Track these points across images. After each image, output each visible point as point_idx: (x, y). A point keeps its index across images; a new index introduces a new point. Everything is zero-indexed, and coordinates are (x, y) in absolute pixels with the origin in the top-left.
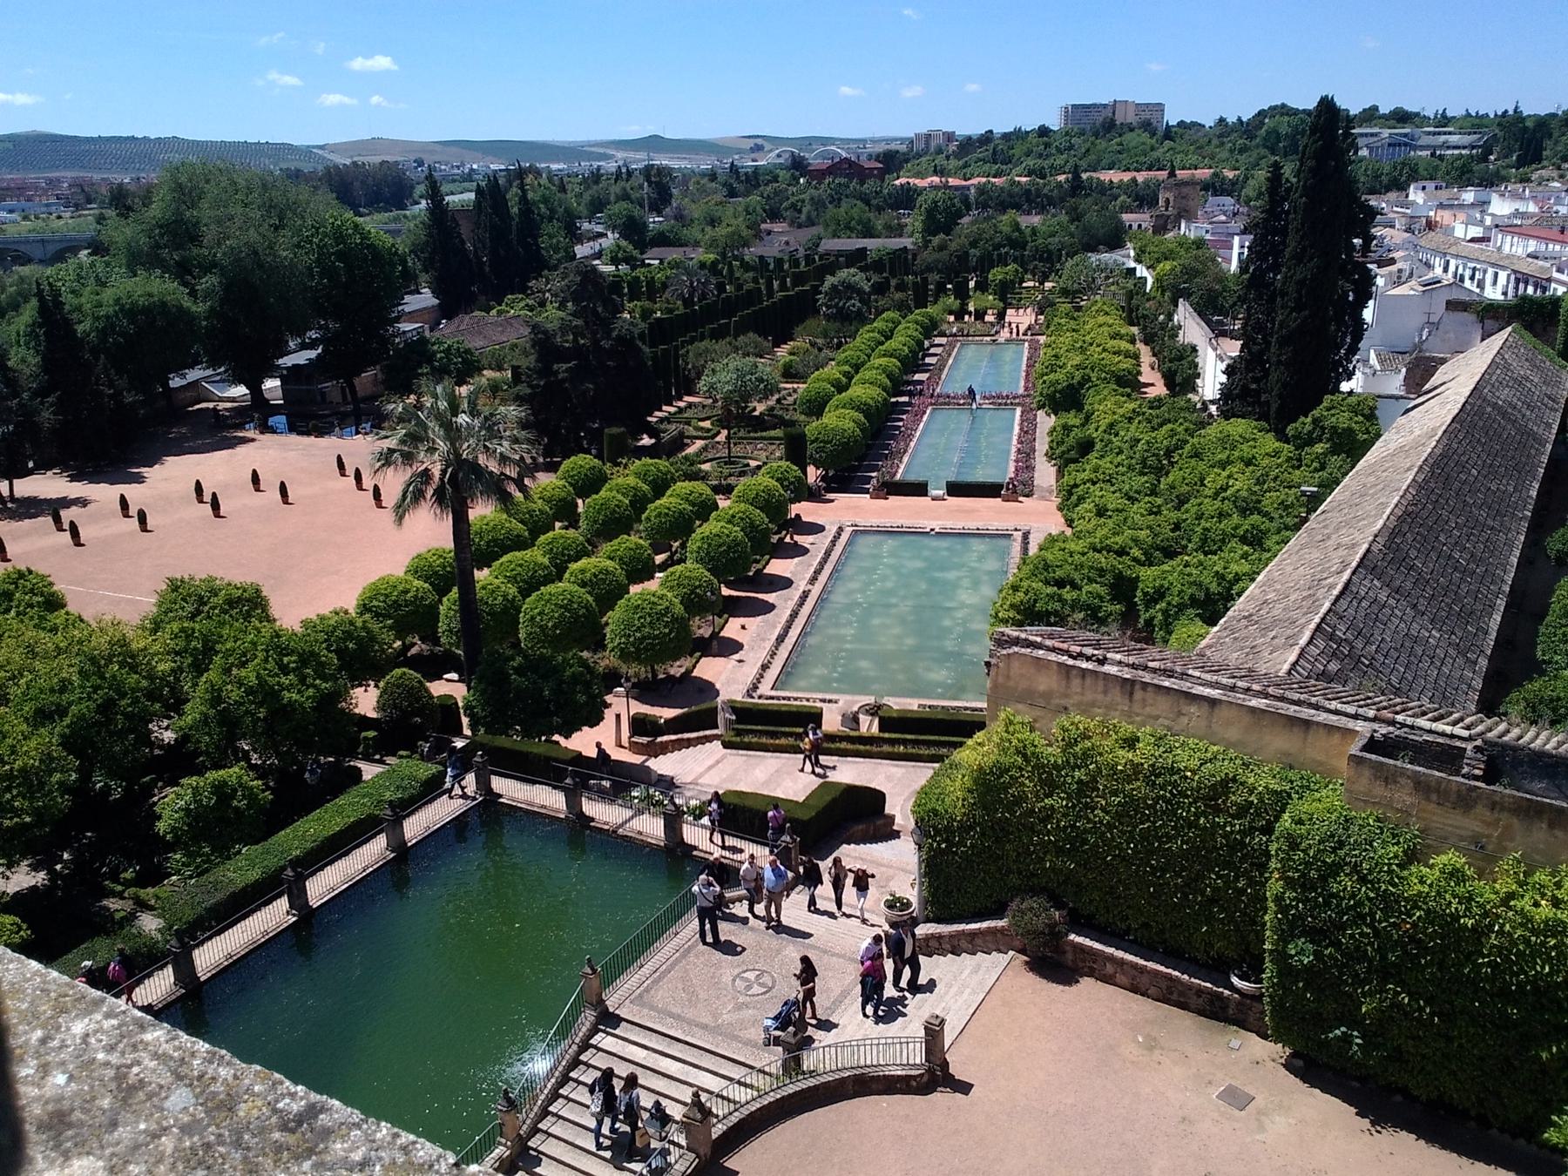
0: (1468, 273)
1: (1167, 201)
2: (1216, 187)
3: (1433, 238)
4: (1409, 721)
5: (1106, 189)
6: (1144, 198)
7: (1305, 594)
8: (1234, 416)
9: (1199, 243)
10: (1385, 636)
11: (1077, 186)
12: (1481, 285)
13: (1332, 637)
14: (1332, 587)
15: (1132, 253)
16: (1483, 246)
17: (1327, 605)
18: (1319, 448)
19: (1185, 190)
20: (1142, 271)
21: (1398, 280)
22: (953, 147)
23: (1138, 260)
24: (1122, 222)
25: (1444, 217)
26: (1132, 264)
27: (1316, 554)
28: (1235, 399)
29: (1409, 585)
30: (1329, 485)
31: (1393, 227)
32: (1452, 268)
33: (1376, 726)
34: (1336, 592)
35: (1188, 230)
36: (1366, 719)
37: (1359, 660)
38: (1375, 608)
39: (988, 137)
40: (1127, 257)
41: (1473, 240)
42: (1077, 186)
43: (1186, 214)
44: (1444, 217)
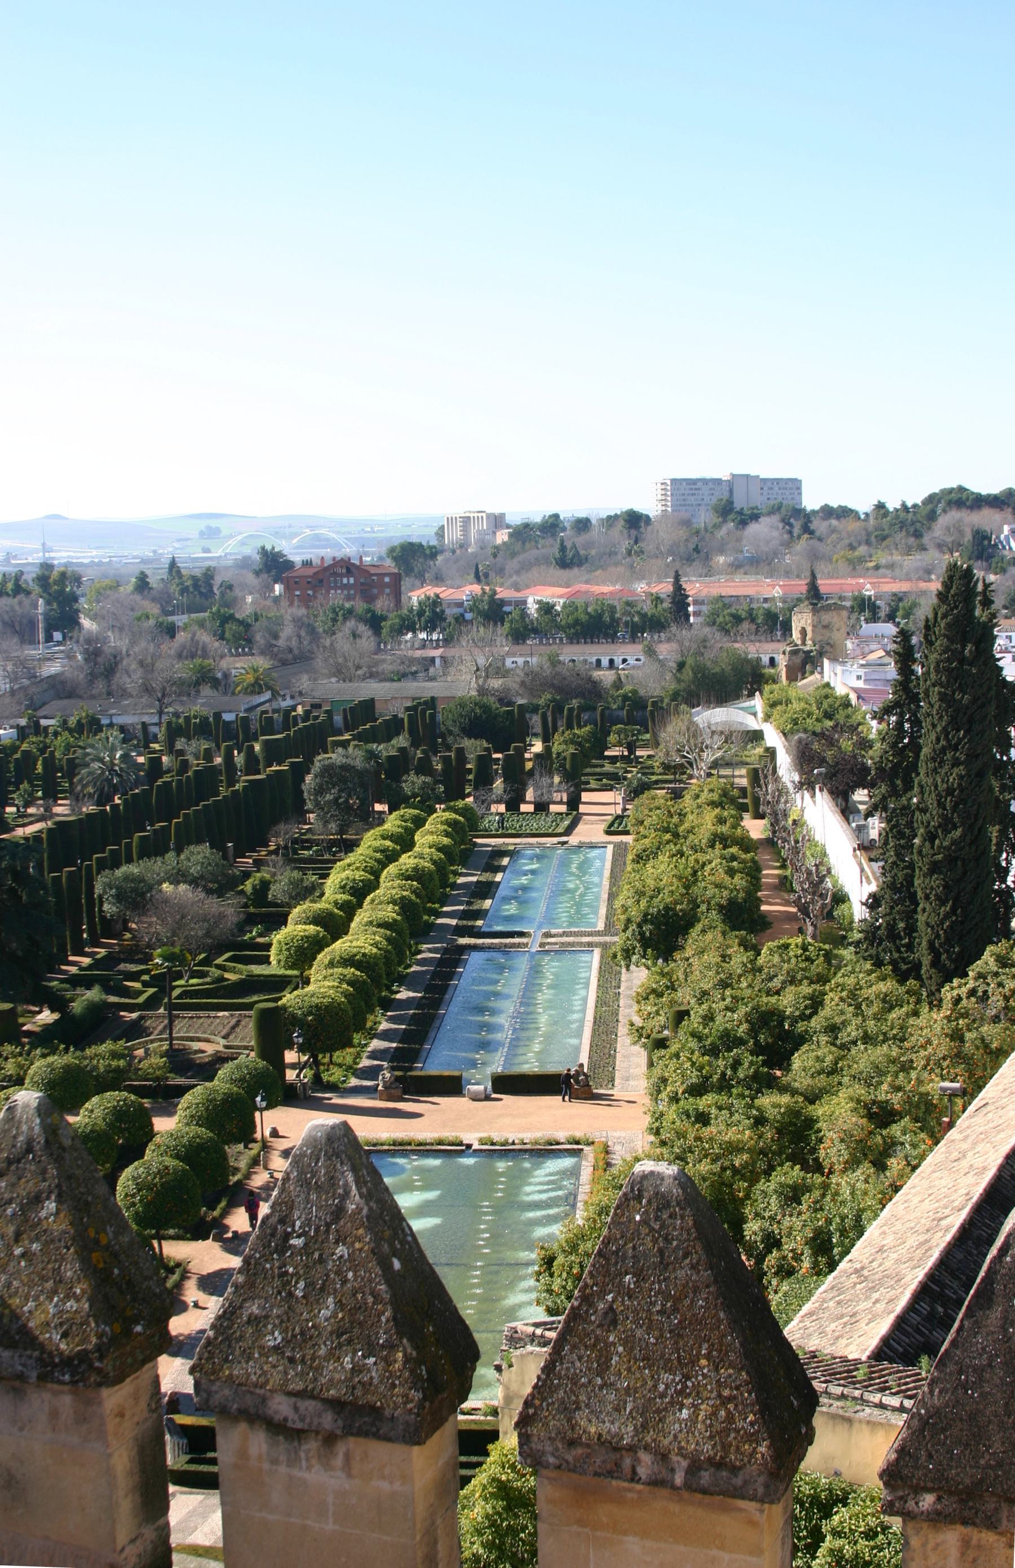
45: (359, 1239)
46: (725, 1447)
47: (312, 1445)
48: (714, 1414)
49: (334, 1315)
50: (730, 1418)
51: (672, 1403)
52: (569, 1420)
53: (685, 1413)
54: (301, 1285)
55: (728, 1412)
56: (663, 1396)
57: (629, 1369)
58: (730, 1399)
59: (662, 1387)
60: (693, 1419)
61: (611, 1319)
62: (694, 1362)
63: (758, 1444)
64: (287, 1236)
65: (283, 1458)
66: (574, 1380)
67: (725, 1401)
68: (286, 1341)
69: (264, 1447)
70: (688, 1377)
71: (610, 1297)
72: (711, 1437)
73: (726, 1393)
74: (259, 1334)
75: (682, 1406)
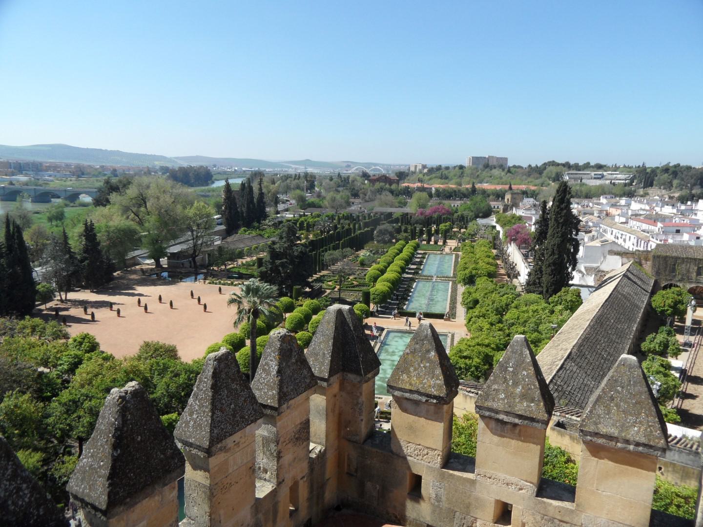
0: (620, 236)
1: (508, 200)
2: (525, 194)
3: (608, 220)
4: (570, 417)
5: (484, 192)
6: (500, 196)
7: (549, 367)
8: (531, 292)
9: (520, 218)
10: (576, 383)
11: (474, 190)
12: (625, 241)
13: (556, 384)
14: (557, 365)
15: (495, 220)
16: (625, 225)
17: (555, 372)
18: (560, 307)
19: (515, 196)
20: (498, 228)
21: (593, 239)
22: (426, 171)
23: (497, 222)
24: (490, 206)
25: (613, 211)
26: (494, 224)
27: (554, 352)
28: (532, 285)
29: (584, 365)
30: (564, 321)
31: (592, 214)
32: (614, 234)
33: (560, 418)
34: (558, 368)
35: (519, 212)
36: (557, 416)
37: (565, 393)
38: (572, 373)
39: (439, 168)
40: (492, 220)
41: (622, 223)
42: (474, 190)
43: (515, 205)
44: (613, 211)
45: (530, 370)
46: (649, 440)
47: (509, 426)
48: (646, 430)
49: (521, 391)
50: (651, 431)
51: (631, 425)
52: (597, 427)
53: (636, 429)
54: (511, 381)
55: (651, 430)
56: (629, 423)
57: (617, 414)
58: (651, 426)
59: (628, 420)
60: (639, 431)
61: (612, 399)
62: (640, 414)
63: (661, 440)
64: (507, 367)
65: (499, 429)
66: (599, 416)
67: (650, 426)
68: (506, 397)
69: (494, 426)
70: (637, 418)
71: (612, 393)
72: (644, 436)
73: (650, 424)
74: (497, 394)
75: (635, 426)
